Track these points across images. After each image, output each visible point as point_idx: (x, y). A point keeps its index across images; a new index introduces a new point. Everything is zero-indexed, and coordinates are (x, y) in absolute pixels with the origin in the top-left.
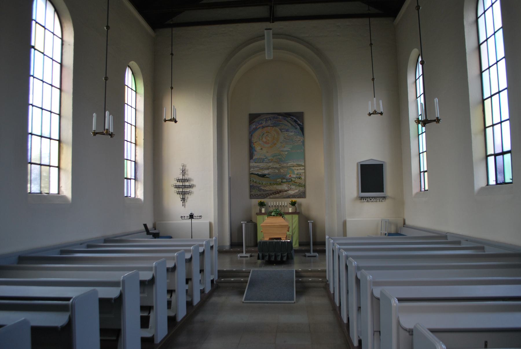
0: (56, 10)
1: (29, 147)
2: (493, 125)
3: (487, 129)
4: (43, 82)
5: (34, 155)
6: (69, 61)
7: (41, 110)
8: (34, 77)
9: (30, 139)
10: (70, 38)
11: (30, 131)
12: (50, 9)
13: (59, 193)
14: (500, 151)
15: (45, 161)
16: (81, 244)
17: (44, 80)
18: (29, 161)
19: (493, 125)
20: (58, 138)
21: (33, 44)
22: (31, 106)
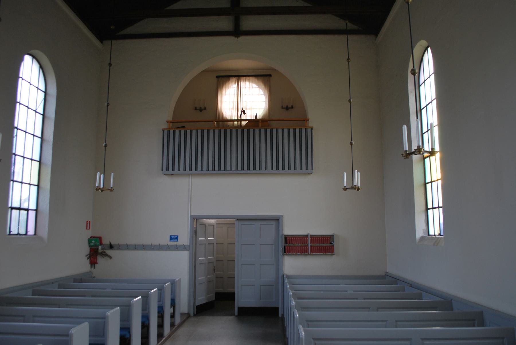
0: (41, 67)
1: (12, 171)
2: (431, 182)
3: (427, 185)
4: (28, 108)
5: (15, 201)
6: (47, 184)
7: (22, 158)
8: (20, 104)
9: (13, 159)
10: (53, 90)
11: (14, 152)
12: (36, 66)
13: (35, 234)
14: (437, 206)
15: (25, 206)
16: (53, 283)
17: (29, 107)
18: (12, 179)
19: (431, 182)
20: (38, 160)
21: (16, 125)
22: (18, 104)
